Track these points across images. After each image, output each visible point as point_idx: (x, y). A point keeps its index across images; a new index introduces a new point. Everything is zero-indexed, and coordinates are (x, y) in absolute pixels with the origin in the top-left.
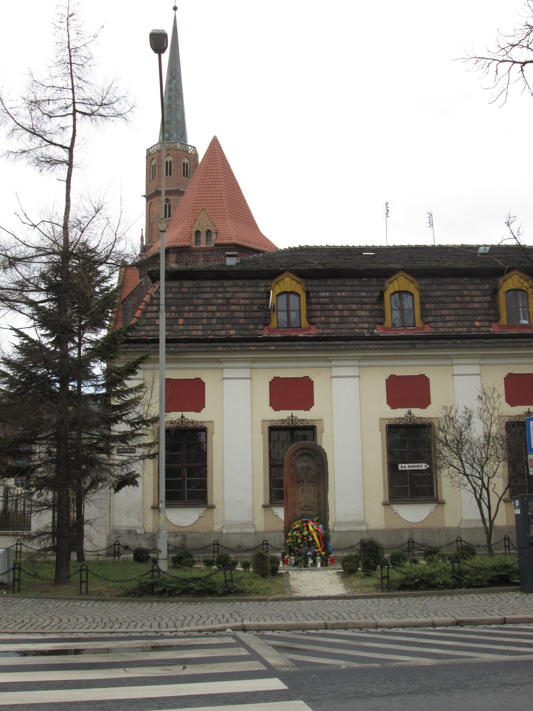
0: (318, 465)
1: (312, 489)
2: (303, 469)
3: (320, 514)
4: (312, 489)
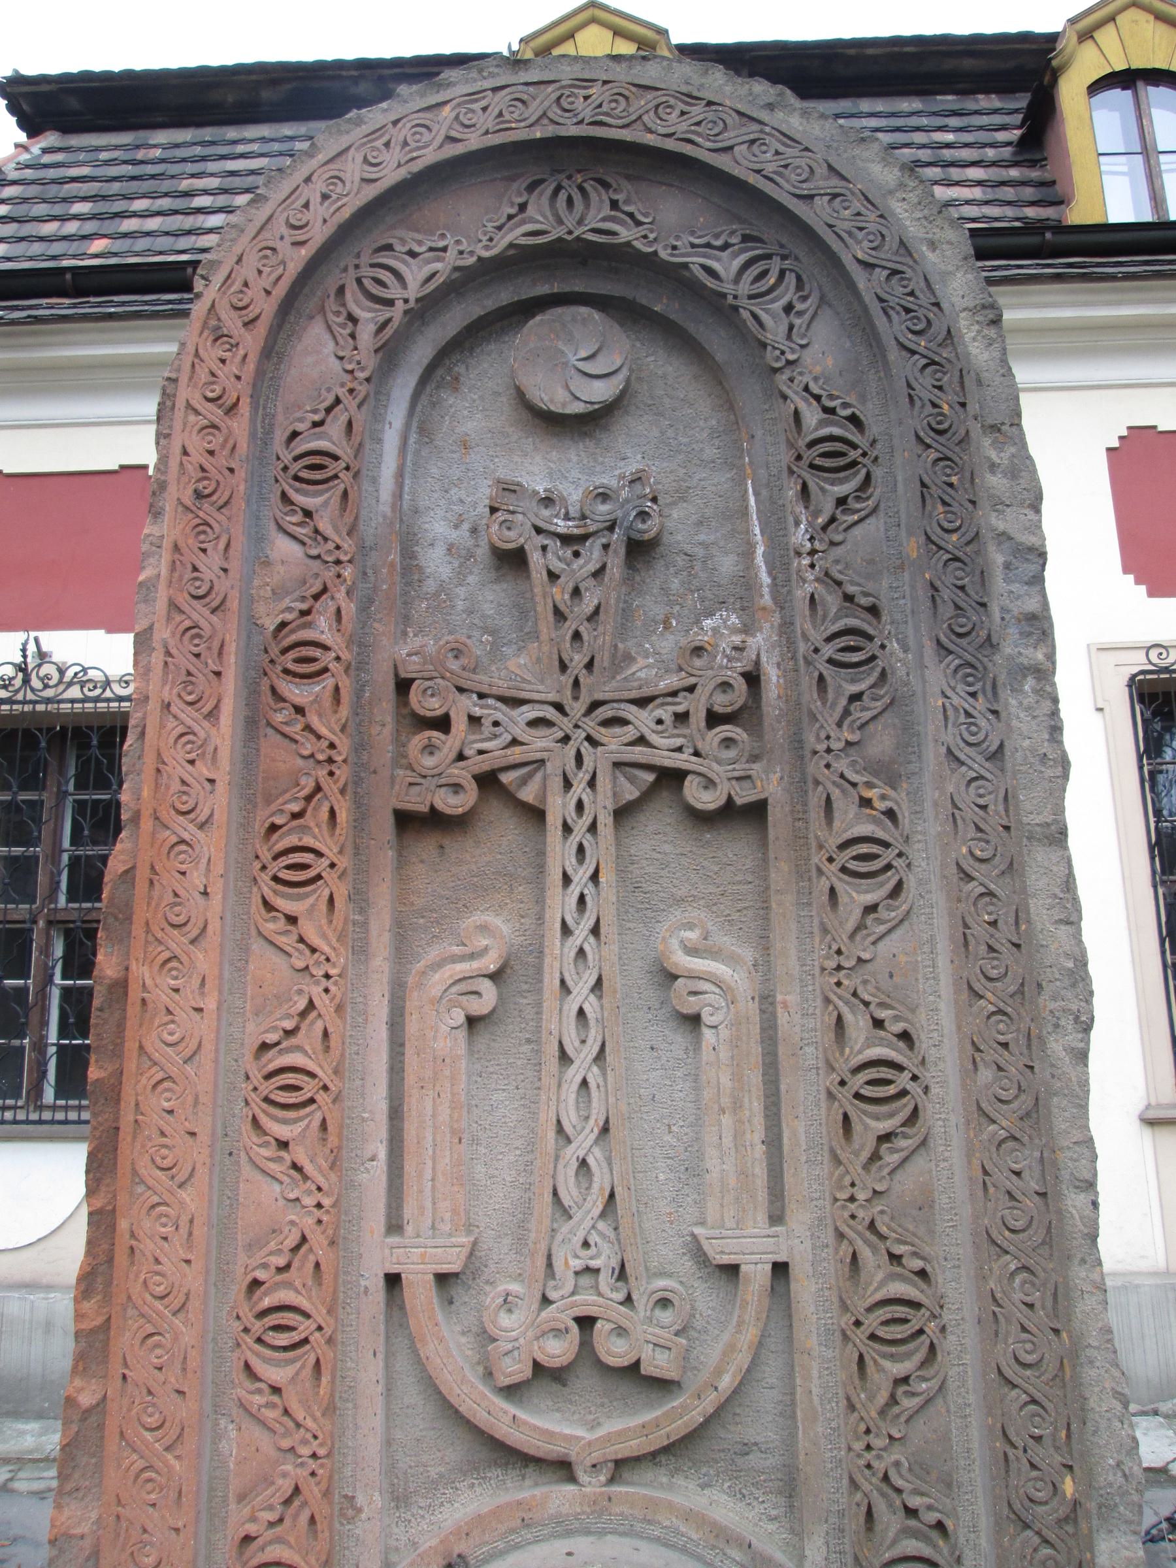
0: (835, 456)
1: (722, 973)
2: (512, 561)
4: (722, 973)
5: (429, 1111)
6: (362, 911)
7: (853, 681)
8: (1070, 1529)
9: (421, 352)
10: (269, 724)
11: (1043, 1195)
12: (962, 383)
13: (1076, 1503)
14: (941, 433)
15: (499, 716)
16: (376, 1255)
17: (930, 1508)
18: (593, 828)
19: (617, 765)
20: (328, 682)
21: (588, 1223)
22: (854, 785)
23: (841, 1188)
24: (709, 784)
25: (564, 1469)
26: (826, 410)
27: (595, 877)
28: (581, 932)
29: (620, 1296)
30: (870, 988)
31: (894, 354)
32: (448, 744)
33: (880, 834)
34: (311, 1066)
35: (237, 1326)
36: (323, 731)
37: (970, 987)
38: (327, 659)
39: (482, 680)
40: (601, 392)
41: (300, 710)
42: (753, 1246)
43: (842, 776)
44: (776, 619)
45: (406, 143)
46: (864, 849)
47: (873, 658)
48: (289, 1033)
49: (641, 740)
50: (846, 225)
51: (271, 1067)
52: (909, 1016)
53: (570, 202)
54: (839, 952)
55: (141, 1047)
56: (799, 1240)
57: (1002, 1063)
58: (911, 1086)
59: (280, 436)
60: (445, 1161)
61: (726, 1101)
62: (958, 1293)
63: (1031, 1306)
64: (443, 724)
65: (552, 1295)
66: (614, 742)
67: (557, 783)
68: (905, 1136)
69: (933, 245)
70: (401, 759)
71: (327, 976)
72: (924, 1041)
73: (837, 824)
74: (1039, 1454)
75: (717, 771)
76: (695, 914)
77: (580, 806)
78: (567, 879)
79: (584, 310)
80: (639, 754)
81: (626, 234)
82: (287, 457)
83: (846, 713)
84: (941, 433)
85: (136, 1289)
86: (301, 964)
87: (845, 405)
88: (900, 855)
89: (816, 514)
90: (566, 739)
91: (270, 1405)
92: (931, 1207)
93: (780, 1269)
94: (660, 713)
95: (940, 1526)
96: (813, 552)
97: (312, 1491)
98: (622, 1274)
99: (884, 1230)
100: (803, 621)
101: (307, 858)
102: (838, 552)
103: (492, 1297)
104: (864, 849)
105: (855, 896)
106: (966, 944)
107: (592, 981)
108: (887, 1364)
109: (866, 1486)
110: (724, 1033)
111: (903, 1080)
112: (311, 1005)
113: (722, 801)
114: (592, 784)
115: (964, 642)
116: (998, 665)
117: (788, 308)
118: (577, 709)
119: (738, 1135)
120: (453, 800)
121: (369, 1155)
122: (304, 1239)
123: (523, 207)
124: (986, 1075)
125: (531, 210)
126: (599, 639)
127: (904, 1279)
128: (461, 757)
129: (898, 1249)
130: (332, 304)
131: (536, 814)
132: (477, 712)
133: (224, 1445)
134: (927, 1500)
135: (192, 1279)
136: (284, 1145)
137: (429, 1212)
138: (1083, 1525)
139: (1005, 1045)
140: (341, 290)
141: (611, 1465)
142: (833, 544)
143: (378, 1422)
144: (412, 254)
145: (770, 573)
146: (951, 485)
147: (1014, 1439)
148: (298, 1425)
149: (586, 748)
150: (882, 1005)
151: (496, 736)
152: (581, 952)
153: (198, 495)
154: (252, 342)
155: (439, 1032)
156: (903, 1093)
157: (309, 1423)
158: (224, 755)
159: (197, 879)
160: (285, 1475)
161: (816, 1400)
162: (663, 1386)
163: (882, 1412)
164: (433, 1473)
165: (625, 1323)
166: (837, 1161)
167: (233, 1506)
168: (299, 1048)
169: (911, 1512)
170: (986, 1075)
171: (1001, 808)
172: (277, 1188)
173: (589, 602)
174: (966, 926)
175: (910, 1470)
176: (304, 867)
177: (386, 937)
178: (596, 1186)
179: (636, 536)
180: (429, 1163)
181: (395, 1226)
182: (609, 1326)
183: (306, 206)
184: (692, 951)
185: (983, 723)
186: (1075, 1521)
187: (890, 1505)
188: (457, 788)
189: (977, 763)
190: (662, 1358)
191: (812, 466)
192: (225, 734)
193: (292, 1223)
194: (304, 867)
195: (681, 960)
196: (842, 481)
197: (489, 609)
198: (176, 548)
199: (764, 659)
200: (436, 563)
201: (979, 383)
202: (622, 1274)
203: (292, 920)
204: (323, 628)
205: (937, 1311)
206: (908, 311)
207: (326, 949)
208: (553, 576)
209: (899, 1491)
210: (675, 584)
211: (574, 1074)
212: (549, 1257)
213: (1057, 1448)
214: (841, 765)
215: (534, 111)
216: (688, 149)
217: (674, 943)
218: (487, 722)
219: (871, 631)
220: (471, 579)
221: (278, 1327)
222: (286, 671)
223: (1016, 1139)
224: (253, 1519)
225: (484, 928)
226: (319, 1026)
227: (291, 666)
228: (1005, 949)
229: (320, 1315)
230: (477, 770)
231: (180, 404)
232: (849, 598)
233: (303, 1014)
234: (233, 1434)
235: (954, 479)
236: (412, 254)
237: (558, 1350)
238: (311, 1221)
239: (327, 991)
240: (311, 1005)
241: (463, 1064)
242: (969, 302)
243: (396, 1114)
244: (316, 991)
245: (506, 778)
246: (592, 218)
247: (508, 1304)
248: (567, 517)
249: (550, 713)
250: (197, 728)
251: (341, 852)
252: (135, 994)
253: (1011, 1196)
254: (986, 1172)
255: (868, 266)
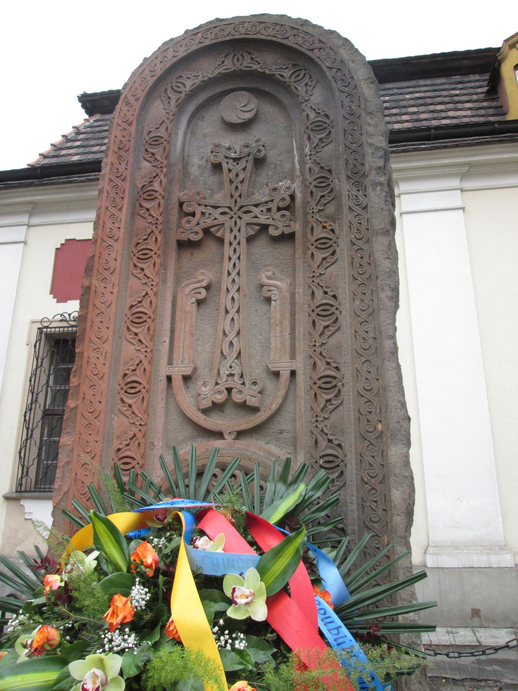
0: (321, 127)
1: (279, 285)
2: (217, 167)
3: (332, 463)
4: (279, 285)
5: (183, 327)
6: (165, 270)
7: (322, 192)
8: (380, 440)
9: (191, 108)
10: (138, 214)
11: (375, 338)
12: (359, 101)
13: (382, 432)
14: (351, 115)
15: (210, 212)
16: (164, 370)
17: (336, 439)
18: (239, 244)
19: (248, 224)
20: (157, 201)
21: (231, 360)
22: (321, 222)
23: (311, 342)
24: (277, 228)
25: (219, 435)
26: (317, 113)
27: (239, 258)
28: (234, 274)
29: (241, 382)
30: (323, 282)
31: (337, 93)
32: (194, 221)
33: (329, 236)
34: (146, 311)
35: (119, 387)
36: (155, 215)
37: (353, 277)
38: (156, 195)
39: (206, 202)
40: (248, 116)
41: (148, 210)
42: (284, 366)
43: (317, 220)
44: (301, 179)
45: (186, 45)
46: (323, 241)
47: (329, 185)
48: (140, 302)
49: (256, 217)
50: (324, 57)
51: (134, 312)
52: (335, 290)
53: (238, 59)
54: (314, 272)
55: (94, 304)
56: (300, 364)
57: (363, 298)
58: (335, 311)
59: (146, 132)
60: (187, 342)
61: (278, 322)
62: (347, 372)
63: (369, 372)
64: (193, 214)
65: (219, 382)
66: (247, 218)
67: (228, 230)
68: (333, 327)
69: (353, 61)
70: (179, 226)
71: (152, 285)
72: (340, 297)
73: (315, 234)
74: (370, 417)
75: (280, 224)
76: (270, 268)
77: (235, 237)
78: (230, 259)
79: (243, 92)
80: (255, 220)
81: (255, 67)
82: (147, 138)
83: (319, 201)
84: (351, 115)
85: (89, 373)
86: (144, 282)
87: (323, 111)
88: (335, 242)
89: (313, 143)
90: (231, 218)
91: (127, 410)
92: (341, 347)
93: (293, 373)
94: (262, 209)
95: (339, 445)
96: (310, 155)
97: (139, 435)
98: (242, 376)
99: (325, 355)
100: (308, 176)
101: (148, 251)
102: (318, 155)
103: (200, 383)
104: (323, 241)
105: (319, 256)
106: (352, 263)
107: (237, 288)
108: (324, 396)
109: (315, 433)
110: (278, 302)
111: (333, 309)
112: (147, 294)
113: (281, 233)
114: (239, 230)
115: (356, 175)
116: (367, 182)
117: (306, 85)
118: (235, 209)
119: (281, 332)
120: (195, 237)
121: (163, 340)
122: (141, 361)
123: (223, 62)
124: (357, 302)
125: (226, 63)
126: (243, 188)
127: (331, 370)
128: (198, 224)
129: (329, 361)
130: (163, 94)
131: (221, 241)
132: (204, 211)
133: (113, 423)
134: (335, 437)
135: (106, 369)
136: (136, 334)
137: (181, 357)
138: (384, 439)
139: (364, 294)
140: (166, 90)
141: (235, 433)
142: (317, 152)
143: (162, 420)
144: (188, 78)
145: (299, 165)
146: (354, 130)
147: (362, 412)
148: (137, 416)
149: (238, 220)
150: (327, 287)
151: (209, 218)
152: (234, 281)
153: (119, 149)
154: (137, 105)
155: (188, 304)
156: (333, 313)
157: (140, 415)
158: (123, 220)
159: (113, 256)
160: (131, 431)
161: (303, 412)
162: (255, 410)
163: (322, 410)
164: (180, 439)
165: (242, 389)
166: (310, 334)
167: (115, 440)
168: (143, 306)
169: (330, 441)
170: (357, 302)
171: (366, 224)
172: (133, 347)
173: (241, 177)
174: (352, 258)
175: (330, 428)
176: (147, 254)
177: (172, 277)
178: (235, 349)
179: (256, 157)
180: (182, 342)
181: (170, 362)
182: (237, 390)
183: (155, 65)
184: (269, 278)
185: (361, 198)
186: (382, 438)
187: (323, 438)
188: (197, 233)
189: (359, 210)
190: (253, 399)
191: (312, 130)
192: (124, 215)
193: (138, 357)
194: (147, 254)
195: (266, 281)
196: (321, 134)
197: (210, 183)
198: (112, 164)
199: (296, 190)
200: (194, 171)
201: (366, 100)
202: (242, 376)
203: (142, 270)
204: (156, 186)
205: (341, 379)
206: (342, 80)
207: (152, 277)
208: (230, 171)
209: (326, 434)
210: (270, 173)
211: (230, 316)
212: (219, 371)
213: (376, 415)
214: (317, 216)
215: (226, 33)
216: (274, 39)
217: (263, 276)
218: (207, 214)
219: (328, 177)
220: (206, 175)
221: (132, 387)
222: (144, 199)
223: (367, 322)
224: (121, 444)
225: (203, 274)
226: (149, 300)
227: (146, 197)
228: (365, 265)
229: (144, 383)
230: (203, 227)
231: (115, 123)
232: (322, 168)
233: (144, 297)
234: (116, 419)
235: (355, 128)
236: (188, 78)
237: (220, 398)
238: (143, 356)
239: (152, 289)
240: (147, 294)
241: (195, 314)
242: (365, 77)
243: (172, 331)
244: (148, 290)
245: (212, 230)
246: (246, 63)
247: (205, 384)
248: (235, 153)
249: (227, 210)
250: (115, 213)
251: (158, 249)
252: (93, 289)
253: (364, 339)
254: (356, 332)
255: (330, 68)
